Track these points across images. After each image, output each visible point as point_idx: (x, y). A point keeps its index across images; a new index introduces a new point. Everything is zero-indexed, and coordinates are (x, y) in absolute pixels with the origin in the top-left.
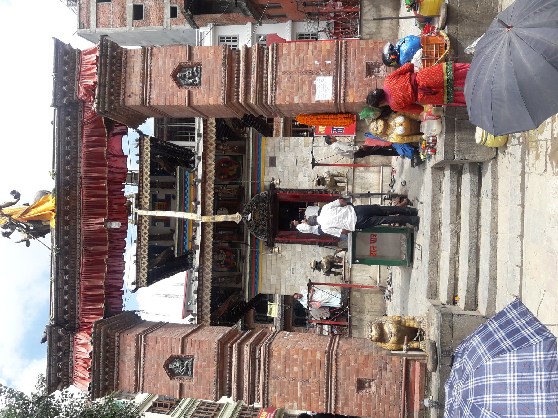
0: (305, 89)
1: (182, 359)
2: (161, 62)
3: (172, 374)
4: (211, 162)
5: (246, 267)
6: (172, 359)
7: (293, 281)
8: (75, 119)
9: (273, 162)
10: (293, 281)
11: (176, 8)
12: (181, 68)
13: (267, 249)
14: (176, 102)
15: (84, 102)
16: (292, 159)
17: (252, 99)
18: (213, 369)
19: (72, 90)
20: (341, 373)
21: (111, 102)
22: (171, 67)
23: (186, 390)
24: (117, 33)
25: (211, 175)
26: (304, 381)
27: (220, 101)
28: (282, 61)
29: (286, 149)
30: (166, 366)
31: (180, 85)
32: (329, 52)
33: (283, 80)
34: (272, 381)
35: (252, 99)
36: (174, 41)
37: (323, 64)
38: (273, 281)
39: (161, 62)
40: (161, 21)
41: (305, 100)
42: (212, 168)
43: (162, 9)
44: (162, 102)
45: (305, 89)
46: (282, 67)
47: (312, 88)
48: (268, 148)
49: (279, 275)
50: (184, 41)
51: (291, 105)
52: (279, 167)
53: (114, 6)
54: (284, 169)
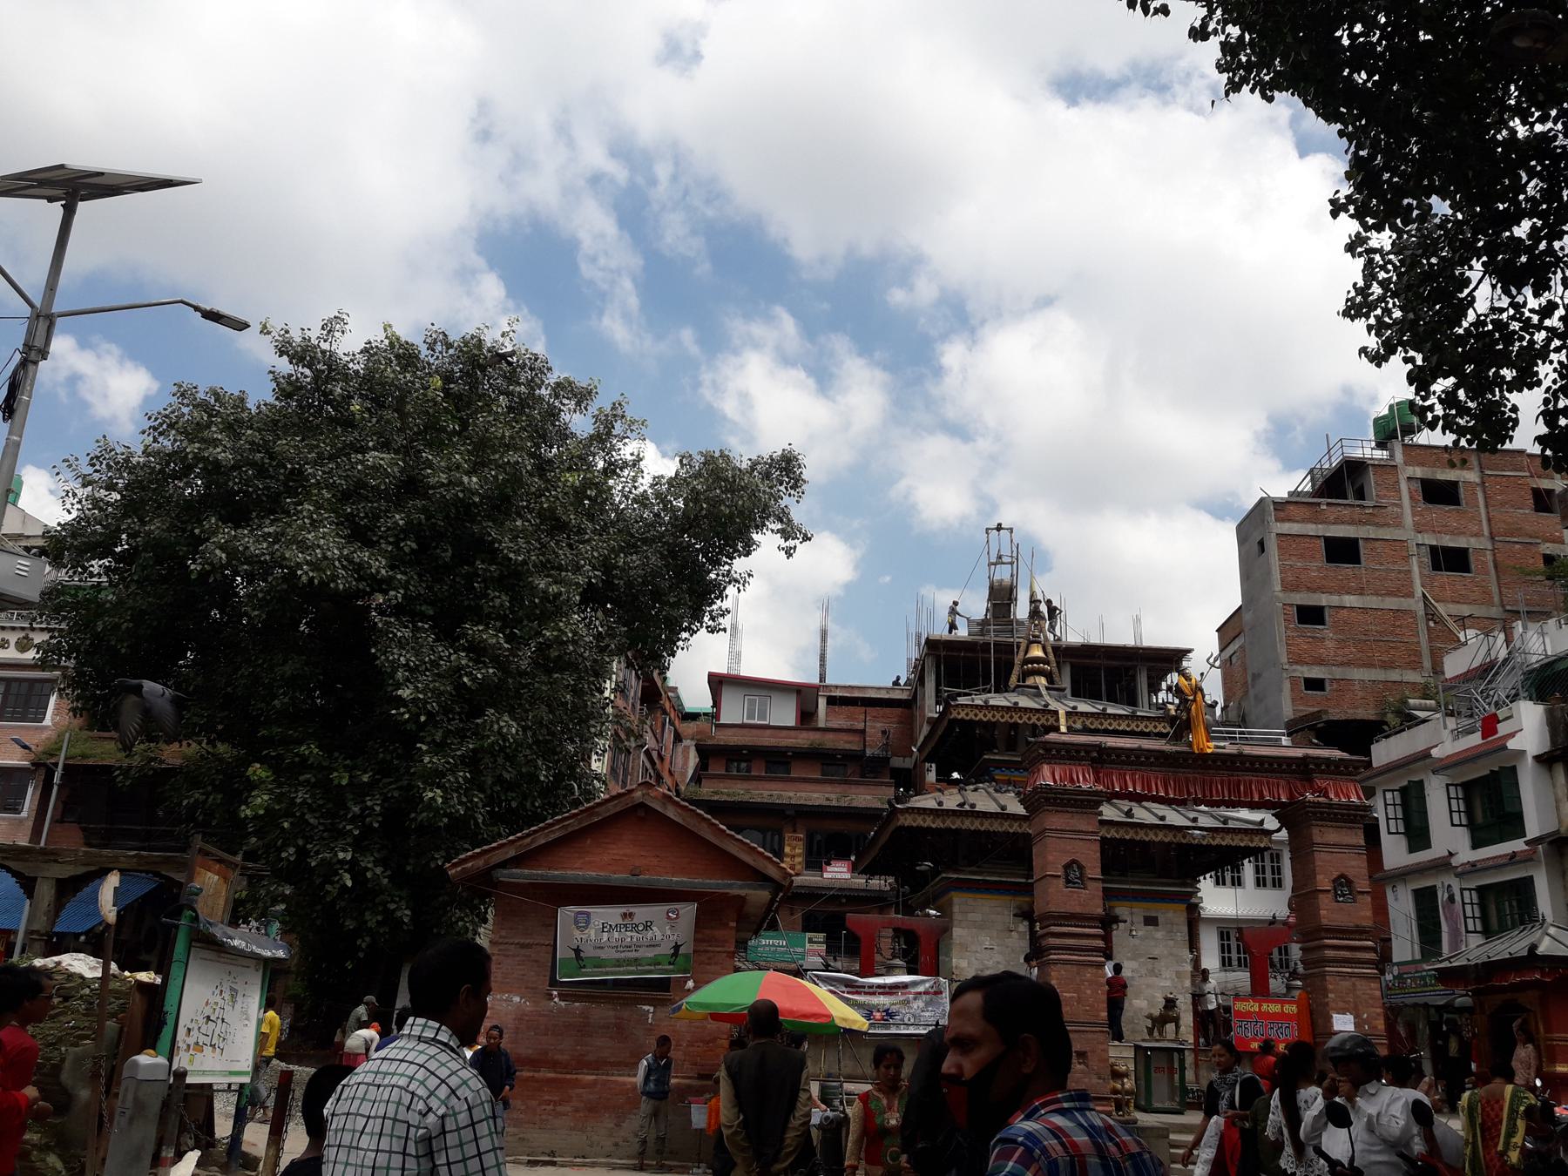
0: (1341, 1005)
1: (1081, 877)
2: (1354, 863)
3: (1067, 867)
4: (1160, 837)
5: (993, 874)
6: (1081, 867)
7: (974, 948)
8: (1294, 772)
9: (1151, 921)
10: (974, 948)
11: (1323, 689)
12: (1349, 883)
13: (1019, 907)
14: (1319, 877)
15: (1310, 781)
16: (1156, 953)
17: (1330, 953)
18: (1078, 910)
19: (1322, 772)
20: (1090, 1036)
21: (1314, 813)
22: (1350, 873)
23: (1055, 881)
24: (1269, 573)
25: (1141, 836)
26: (1079, 1000)
27: (1324, 922)
28: (1363, 982)
29: (1171, 943)
30: (1074, 861)
31: (1334, 881)
32: (1375, 1028)
33: (1346, 984)
34: (1075, 968)
35: (1330, 953)
36: (1256, 677)
37: (1365, 1021)
38: (971, 916)
39: (1354, 863)
40: (1297, 660)
41: (1332, 1005)
42: (1151, 836)
43: (1320, 662)
44: (1318, 863)
45: (1341, 1005)
46: (1358, 983)
47: (1343, 1011)
48: (1170, 915)
49: (981, 926)
50: (1256, 697)
51: (1325, 992)
52: (1141, 931)
53: (1319, 569)
54: (1143, 939)
